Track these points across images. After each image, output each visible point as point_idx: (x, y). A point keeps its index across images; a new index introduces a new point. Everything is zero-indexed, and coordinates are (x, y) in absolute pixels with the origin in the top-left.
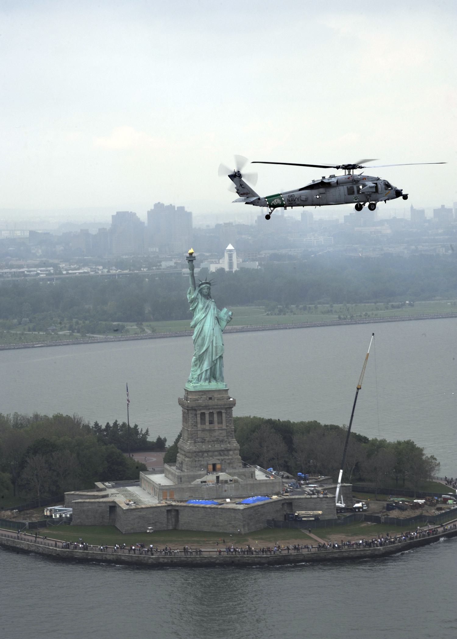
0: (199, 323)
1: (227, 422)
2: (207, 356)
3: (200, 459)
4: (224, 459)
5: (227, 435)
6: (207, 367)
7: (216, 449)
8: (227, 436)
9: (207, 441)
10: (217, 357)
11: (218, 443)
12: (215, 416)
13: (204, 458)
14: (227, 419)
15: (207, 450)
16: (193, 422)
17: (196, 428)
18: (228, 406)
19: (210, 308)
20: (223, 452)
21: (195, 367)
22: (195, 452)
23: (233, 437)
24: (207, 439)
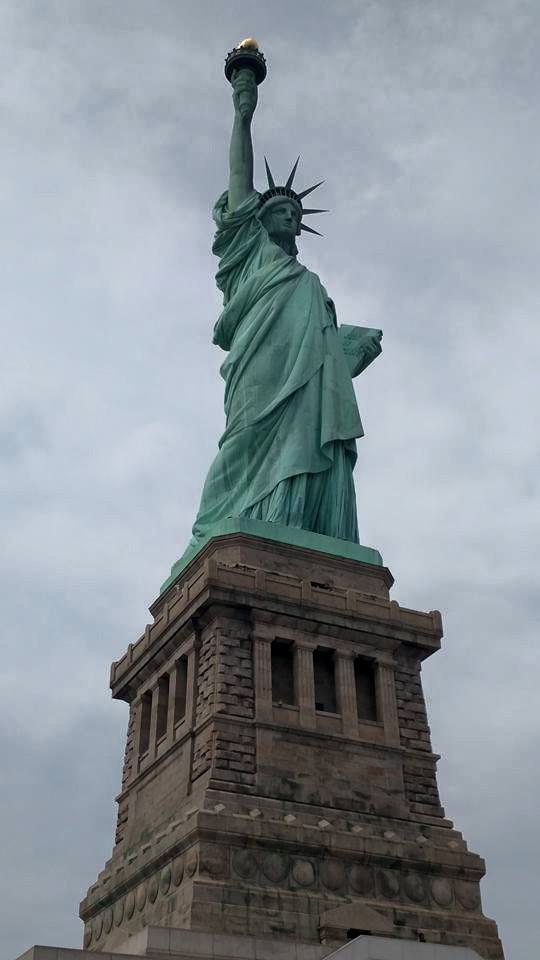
0: (262, 296)
2: (296, 422)
3: (273, 890)
4: (412, 916)
5: (406, 790)
6: (295, 465)
8: (409, 794)
9: (304, 796)
10: (342, 438)
12: (345, 672)
15: (315, 846)
17: (249, 712)
18: (408, 638)
20: (397, 872)
21: (225, 495)
22: (246, 841)
24: (303, 781)
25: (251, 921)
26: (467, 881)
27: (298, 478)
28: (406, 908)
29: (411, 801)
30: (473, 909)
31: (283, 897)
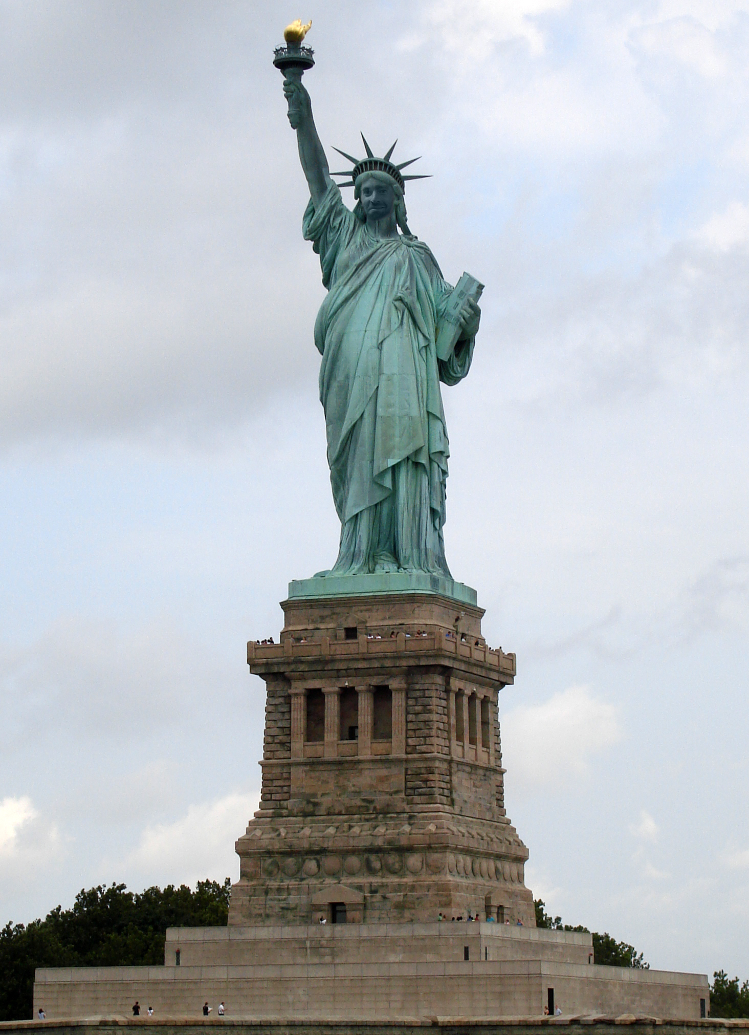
1: (411, 733)
2: (356, 460)
3: (286, 883)
4: (383, 886)
5: (406, 788)
6: (355, 505)
7: (353, 843)
8: (409, 791)
9: (323, 812)
10: (391, 462)
11: (367, 817)
12: (365, 704)
13: (302, 880)
14: (411, 717)
15: (316, 848)
16: (275, 731)
17: (287, 754)
18: (412, 662)
19: (380, 263)
22: (269, 853)
23: (432, 794)
25: (268, 906)
26: (436, 852)
28: (384, 880)
29: (408, 796)
30: (440, 872)
31: (289, 886)
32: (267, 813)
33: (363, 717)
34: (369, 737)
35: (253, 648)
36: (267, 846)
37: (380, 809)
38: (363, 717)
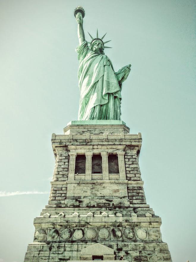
1: (128, 172)
2: (95, 92)
5: (128, 196)
9: (84, 204)
10: (109, 92)
11: (109, 208)
13: (73, 242)
14: (127, 166)
18: (128, 143)
20: (121, 228)
27: (96, 107)
29: (130, 199)
31: (66, 246)
32: (53, 206)
33: (104, 164)
34: (108, 172)
35: (54, 135)
36: (53, 221)
37: (116, 205)
38: (104, 164)
